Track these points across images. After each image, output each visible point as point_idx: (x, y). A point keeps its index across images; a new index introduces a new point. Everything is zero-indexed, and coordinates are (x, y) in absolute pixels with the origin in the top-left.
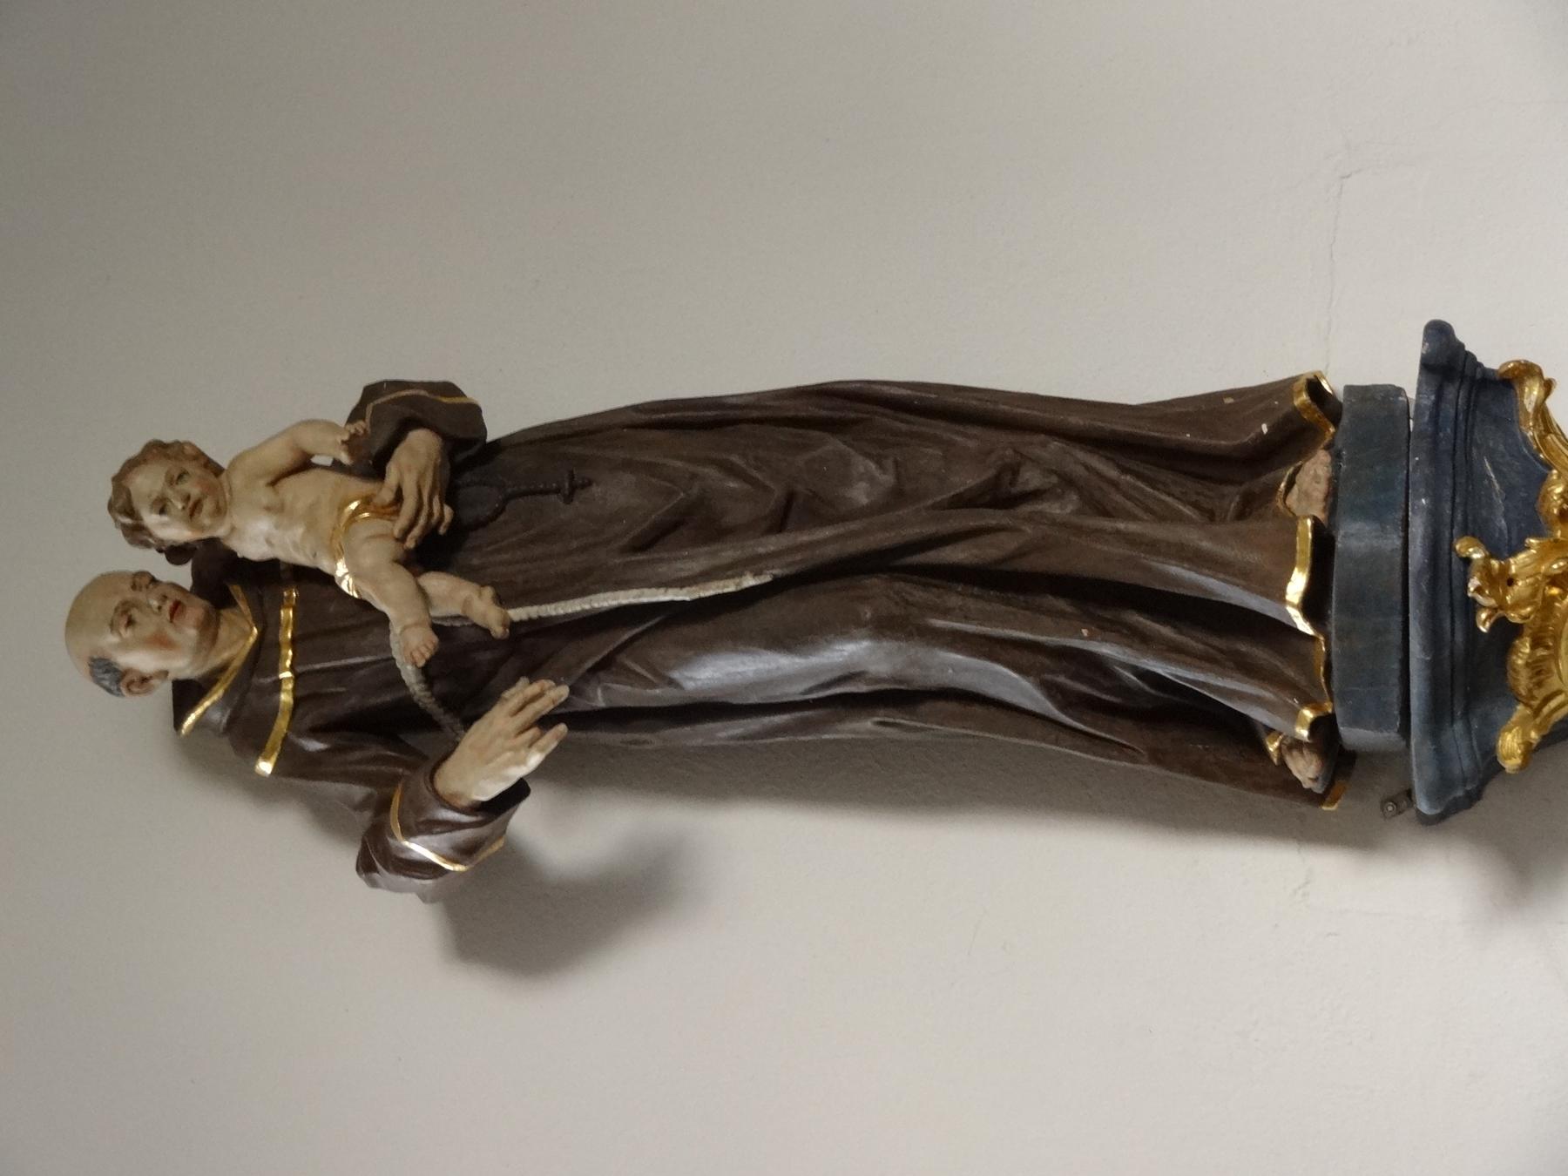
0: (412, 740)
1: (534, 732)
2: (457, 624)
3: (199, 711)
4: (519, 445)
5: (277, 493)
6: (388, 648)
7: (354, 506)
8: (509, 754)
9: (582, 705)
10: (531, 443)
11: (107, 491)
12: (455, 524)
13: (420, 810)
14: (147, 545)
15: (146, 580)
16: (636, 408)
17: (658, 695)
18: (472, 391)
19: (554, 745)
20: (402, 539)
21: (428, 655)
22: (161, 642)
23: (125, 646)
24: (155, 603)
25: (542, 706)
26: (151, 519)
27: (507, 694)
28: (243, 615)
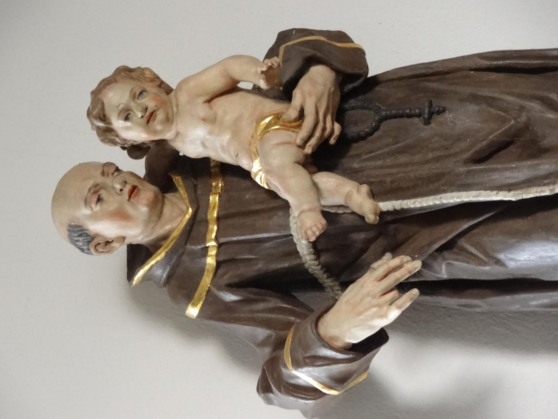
0: (304, 297)
1: (395, 293)
2: (340, 211)
3: (146, 268)
4: (393, 80)
5: (211, 108)
6: (288, 227)
7: (267, 120)
8: (375, 309)
9: (430, 276)
10: (401, 79)
11: (87, 101)
12: (342, 137)
13: (307, 348)
14: (114, 143)
15: (112, 169)
16: (481, 56)
17: (487, 271)
18: (359, 39)
19: (408, 304)
20: (302, 146)
21: (318, 233)
22: (121, 215)
23: (95, 217)
24: (118, 187)
25: (401, 275)
26: (118, 124)
27: (375, 265)
28: (182, 198)
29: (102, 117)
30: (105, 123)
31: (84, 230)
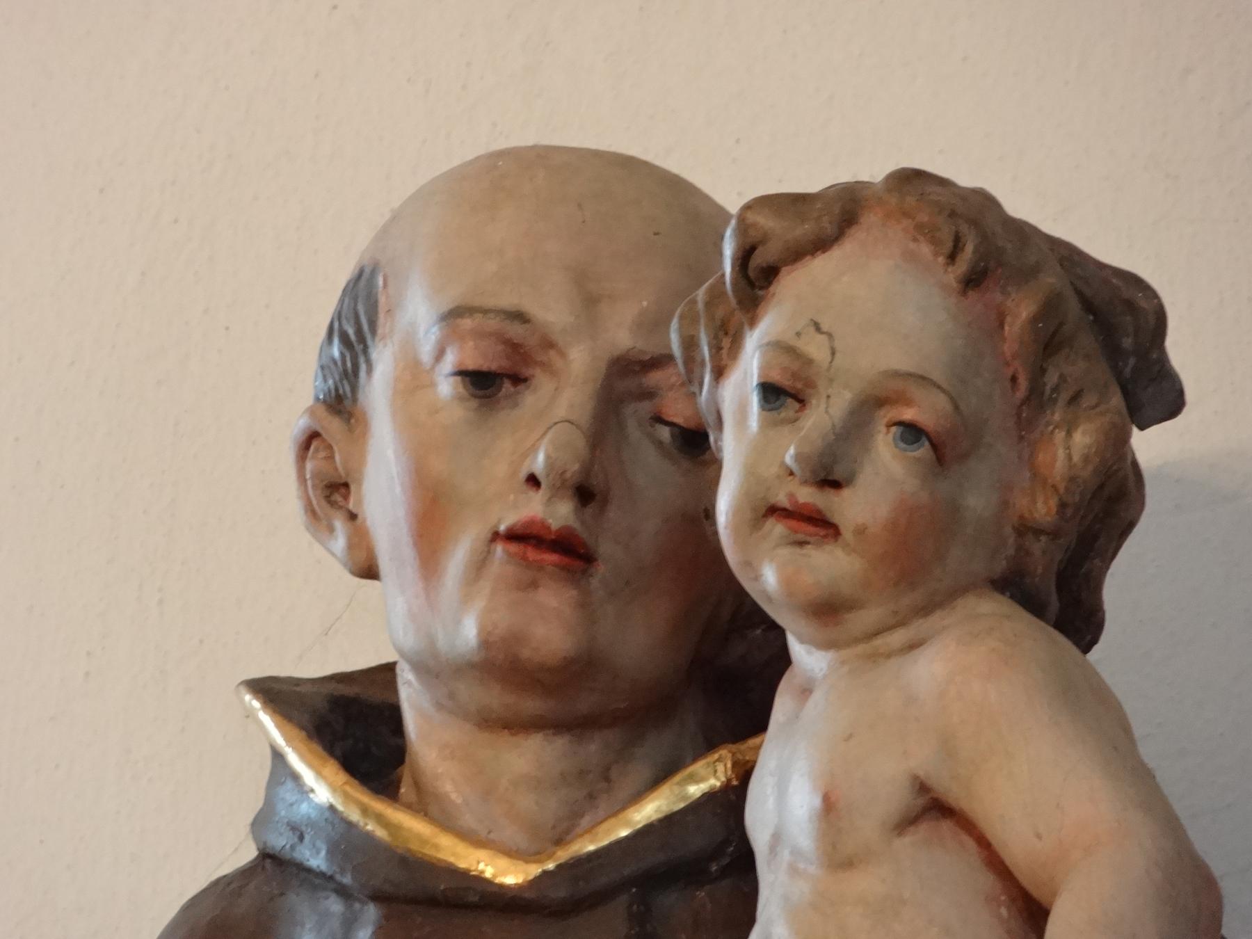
5: (906, 823)
22: (432, 516)
29: (758, 260)
30: (735, 283)
31: (365, 351)
